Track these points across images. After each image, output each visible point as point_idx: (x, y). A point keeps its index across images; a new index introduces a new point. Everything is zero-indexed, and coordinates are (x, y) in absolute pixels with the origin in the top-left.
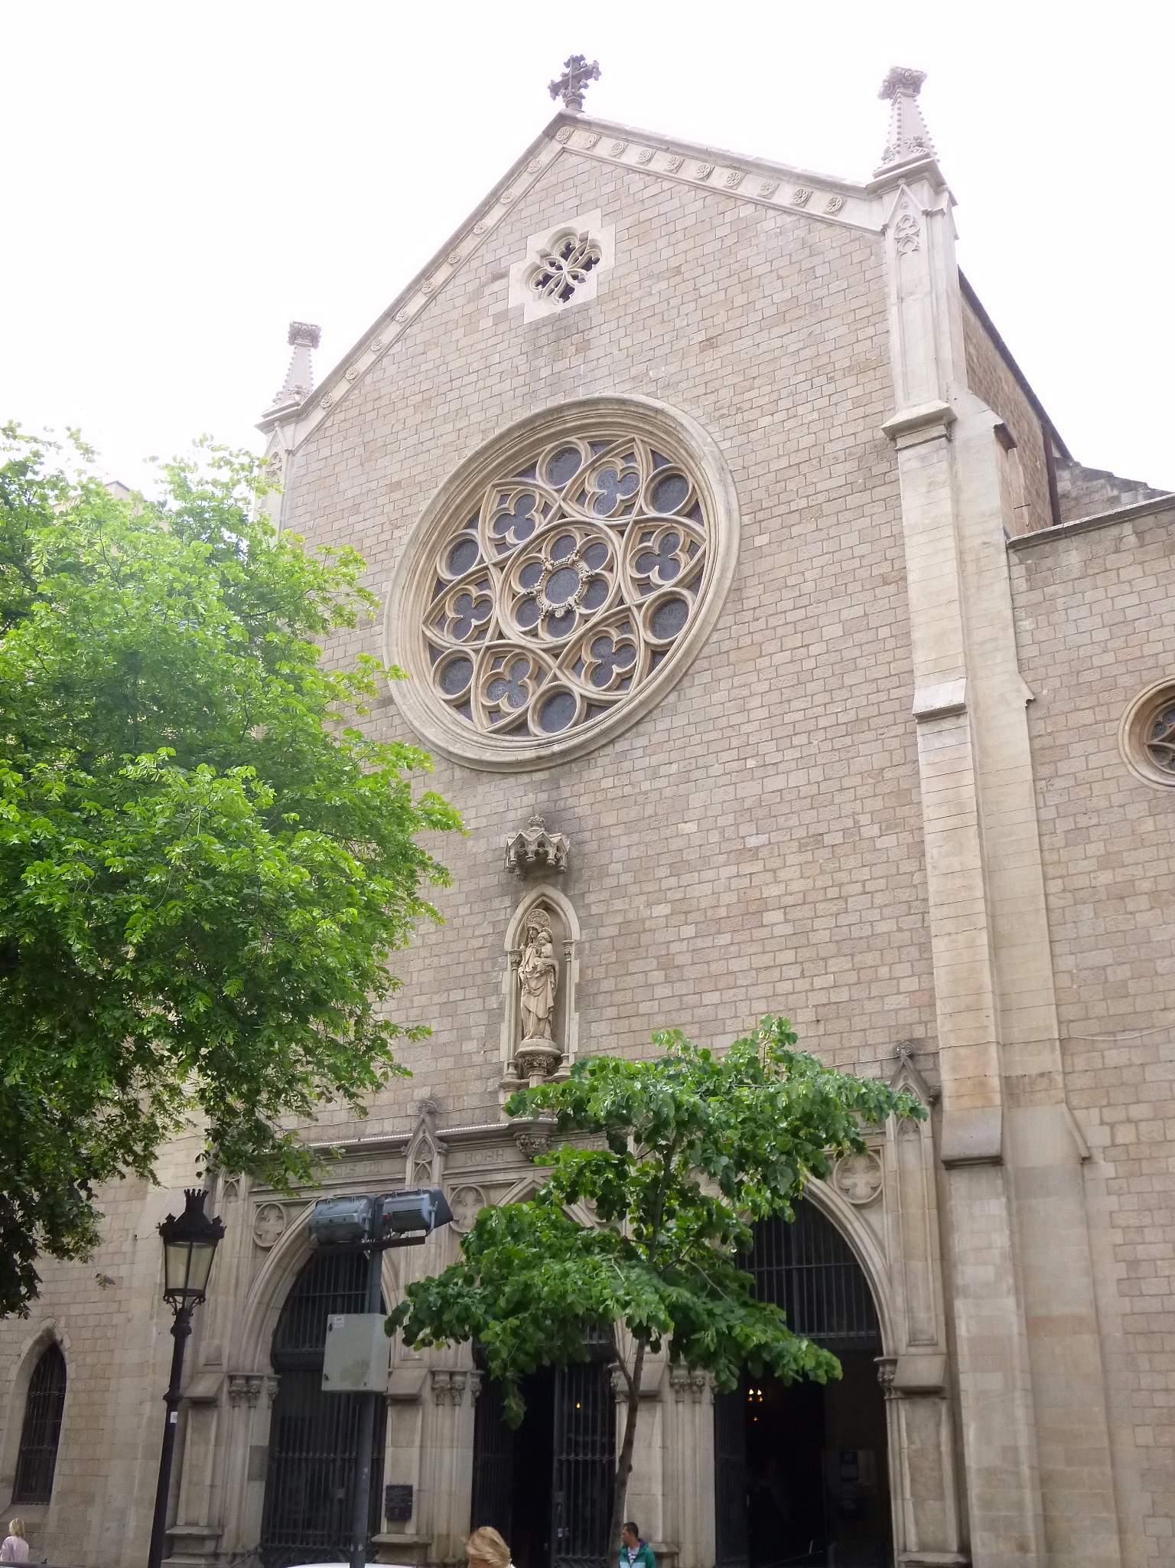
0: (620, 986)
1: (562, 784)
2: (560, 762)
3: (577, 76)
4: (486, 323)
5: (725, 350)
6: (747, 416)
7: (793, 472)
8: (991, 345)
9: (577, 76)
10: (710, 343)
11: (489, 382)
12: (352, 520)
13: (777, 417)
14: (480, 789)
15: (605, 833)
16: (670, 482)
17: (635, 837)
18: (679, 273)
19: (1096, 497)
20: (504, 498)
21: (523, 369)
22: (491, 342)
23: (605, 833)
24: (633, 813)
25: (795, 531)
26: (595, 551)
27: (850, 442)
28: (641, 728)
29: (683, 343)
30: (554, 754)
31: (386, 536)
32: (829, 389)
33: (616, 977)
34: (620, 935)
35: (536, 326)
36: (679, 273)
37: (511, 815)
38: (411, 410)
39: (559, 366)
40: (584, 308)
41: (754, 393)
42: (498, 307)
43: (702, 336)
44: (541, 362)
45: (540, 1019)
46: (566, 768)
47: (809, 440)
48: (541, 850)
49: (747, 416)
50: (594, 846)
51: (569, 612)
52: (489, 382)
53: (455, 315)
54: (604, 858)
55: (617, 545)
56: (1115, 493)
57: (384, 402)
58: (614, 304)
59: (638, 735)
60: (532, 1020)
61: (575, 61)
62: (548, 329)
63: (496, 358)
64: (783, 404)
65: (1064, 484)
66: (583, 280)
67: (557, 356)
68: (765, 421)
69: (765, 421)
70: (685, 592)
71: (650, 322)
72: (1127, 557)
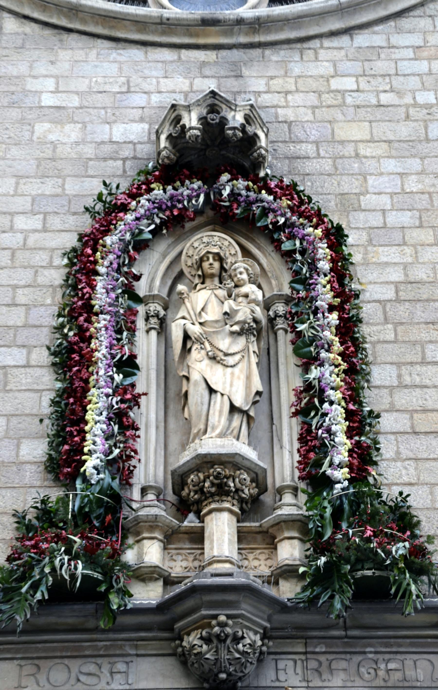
0: (407, 380)
1: (246, 72)
2: (243, 39)
14: (64, 55)
15: (349, 150)
17: (415, 164)
23: (349, 150)
24: (404, 130)
28: (405, 23)
30: (240, 22)
33: (399, 365)
34: (398, 300)
37: (139, 100)
45: (233, 409)
46: (257, 52)
48: (250, 129)
50: (327, 165)
54: (349, 185)
59: (399, 31)
60: (220, 406)
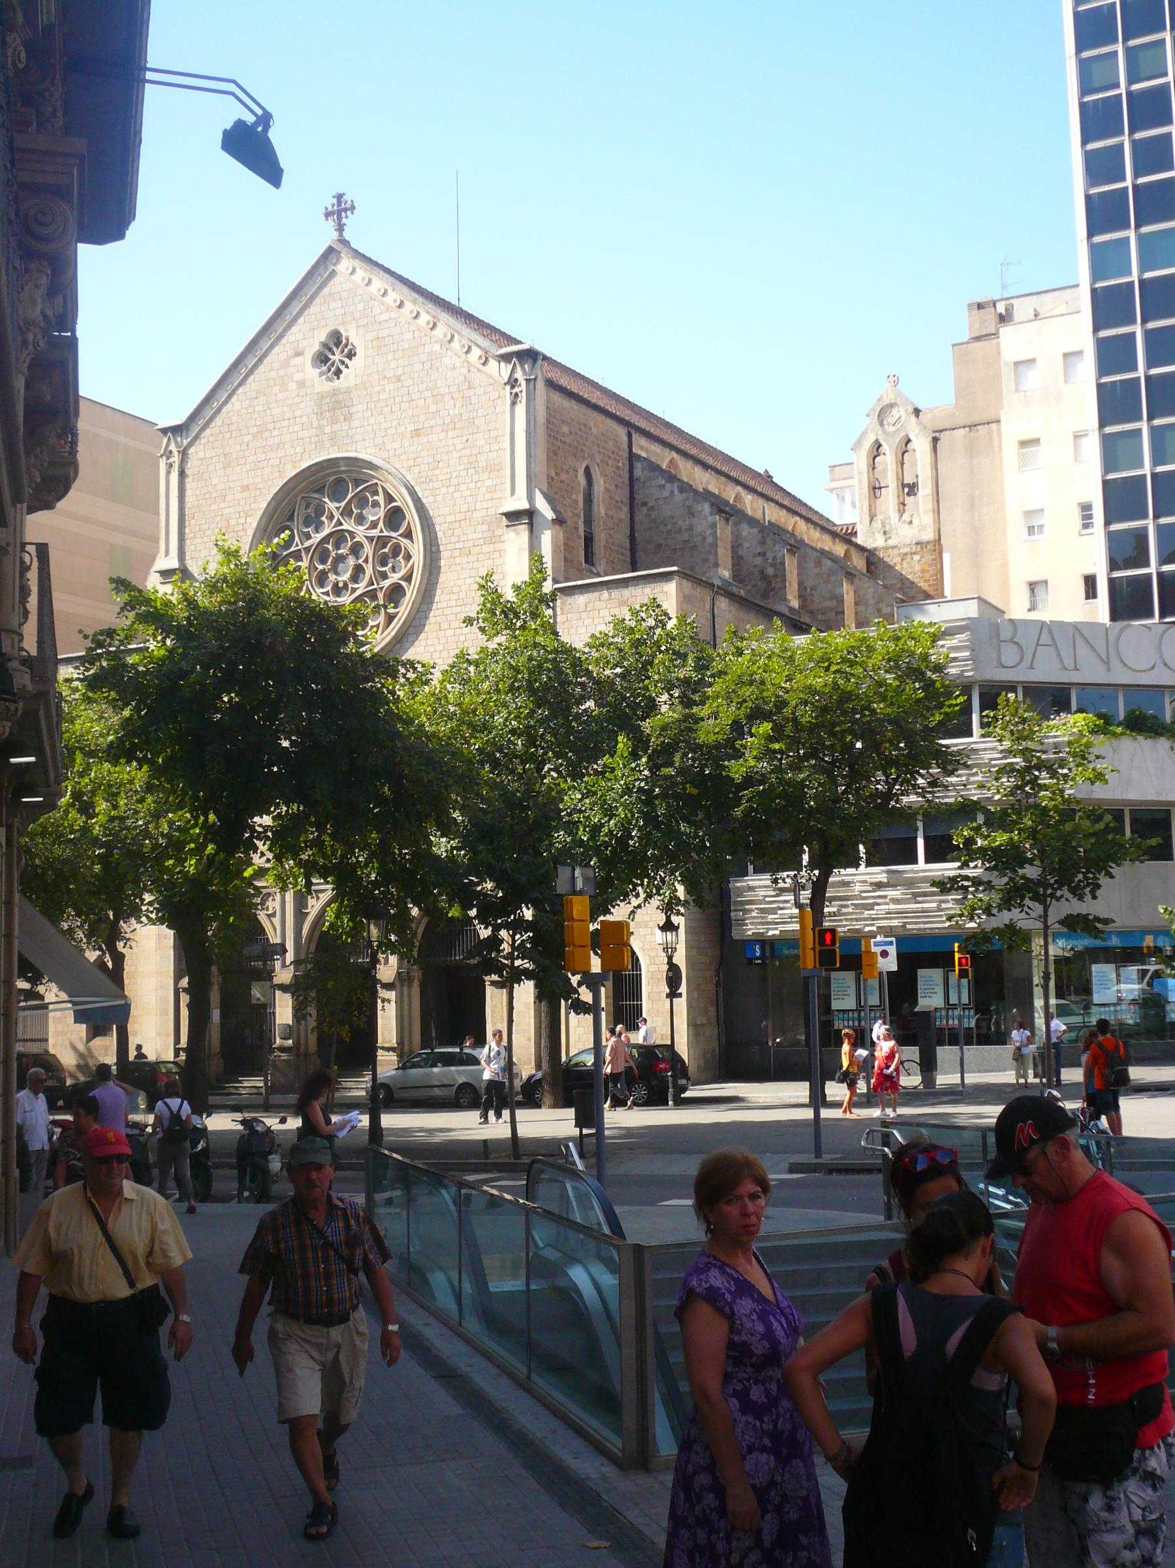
3: (340, 210)
4: (292, 386)
5: (424, 440)
6: (436, 484)
7: (457, 525)
8: (584, 409)
9: (340, 210)
10: (417, 433)
11: (296, 428)
12: (222, 505)
13: (451, 489)
16: (395, 517)
18: (399, 380)
19: (653, 483)
20: (307, 507)
21: (315, 424)
22: (297, 400)
25: (458, 560)
26: (356, 549)
27: (484, 513)
29: (403, 429)
31: (242, 521)
32: (476, 478)
35: (321, 397)
36: (399, 380)
38: (250, 437)
39: (336, 427)
40: (348, 391)
41: (437, 472)
42: (298, 377)
43: (411, 427)
44: (324, 422)
47: (464, 508)
49: (436, 484)
51: (346, 585)
52: (296, 428)
53: (273, 374)
55: (368, 549)
56: (663, 482)
57: (234, 427)
58: (364, 393)
61: (339, 197)
62: (328, 400)
63: (298, 413)
64: (454, 482)
65: (638, 472)
66: (347, 367)
67: (334, 421)
68: (444, 490)
69: (444, 490)
70: (404, 584)
71: (385, 409)
72: (603, 604)
